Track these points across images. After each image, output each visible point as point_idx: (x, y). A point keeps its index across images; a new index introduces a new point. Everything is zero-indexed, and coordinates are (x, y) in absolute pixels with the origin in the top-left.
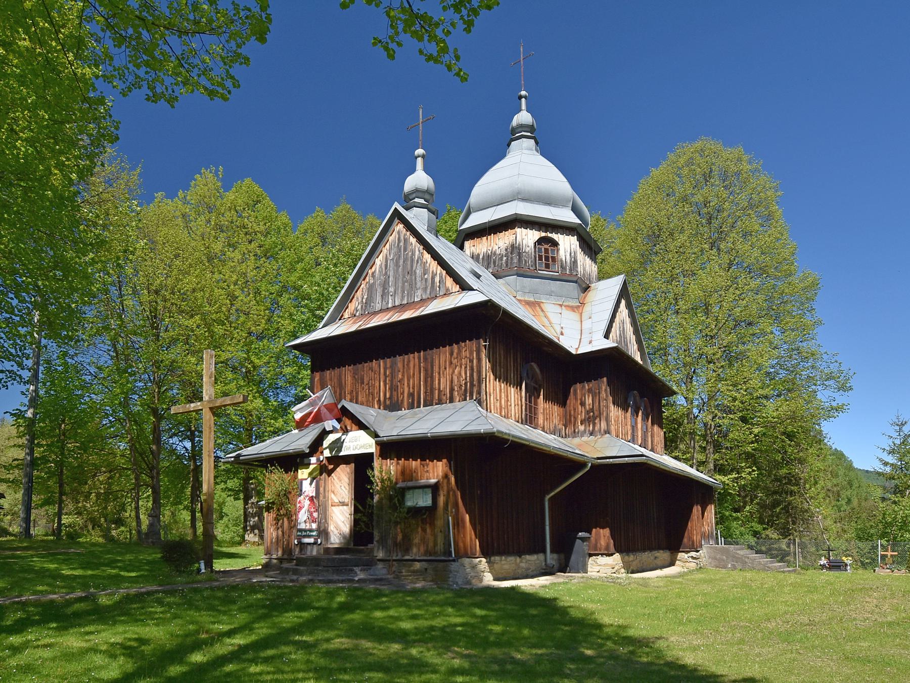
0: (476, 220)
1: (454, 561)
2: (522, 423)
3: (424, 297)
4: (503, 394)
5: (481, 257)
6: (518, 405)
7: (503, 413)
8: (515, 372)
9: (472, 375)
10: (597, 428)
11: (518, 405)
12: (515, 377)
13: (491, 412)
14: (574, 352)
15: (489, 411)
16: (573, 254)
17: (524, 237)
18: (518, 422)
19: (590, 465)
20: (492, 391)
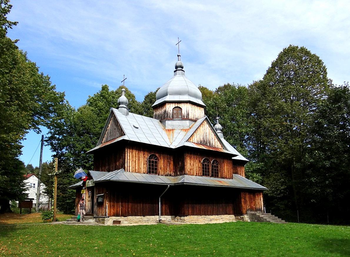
0: (157, 102)
1: (107, 217)
2: (147, 173)
3: (117, 137)
4: (137, 165)
5: (158, 115)
6: (145, 168)
7: (137, 171)
8: (144, 158)
9: (123, 162)
10: (182, 173)
11: (145, 168)
12: (144, 159)
13: (129, 171)
14: (173, 147)
15: (128, 171)
16: (187, 111)
17: (169, 108)
18: (145, 173)
19: (169, 186)
20: (130, 165)
